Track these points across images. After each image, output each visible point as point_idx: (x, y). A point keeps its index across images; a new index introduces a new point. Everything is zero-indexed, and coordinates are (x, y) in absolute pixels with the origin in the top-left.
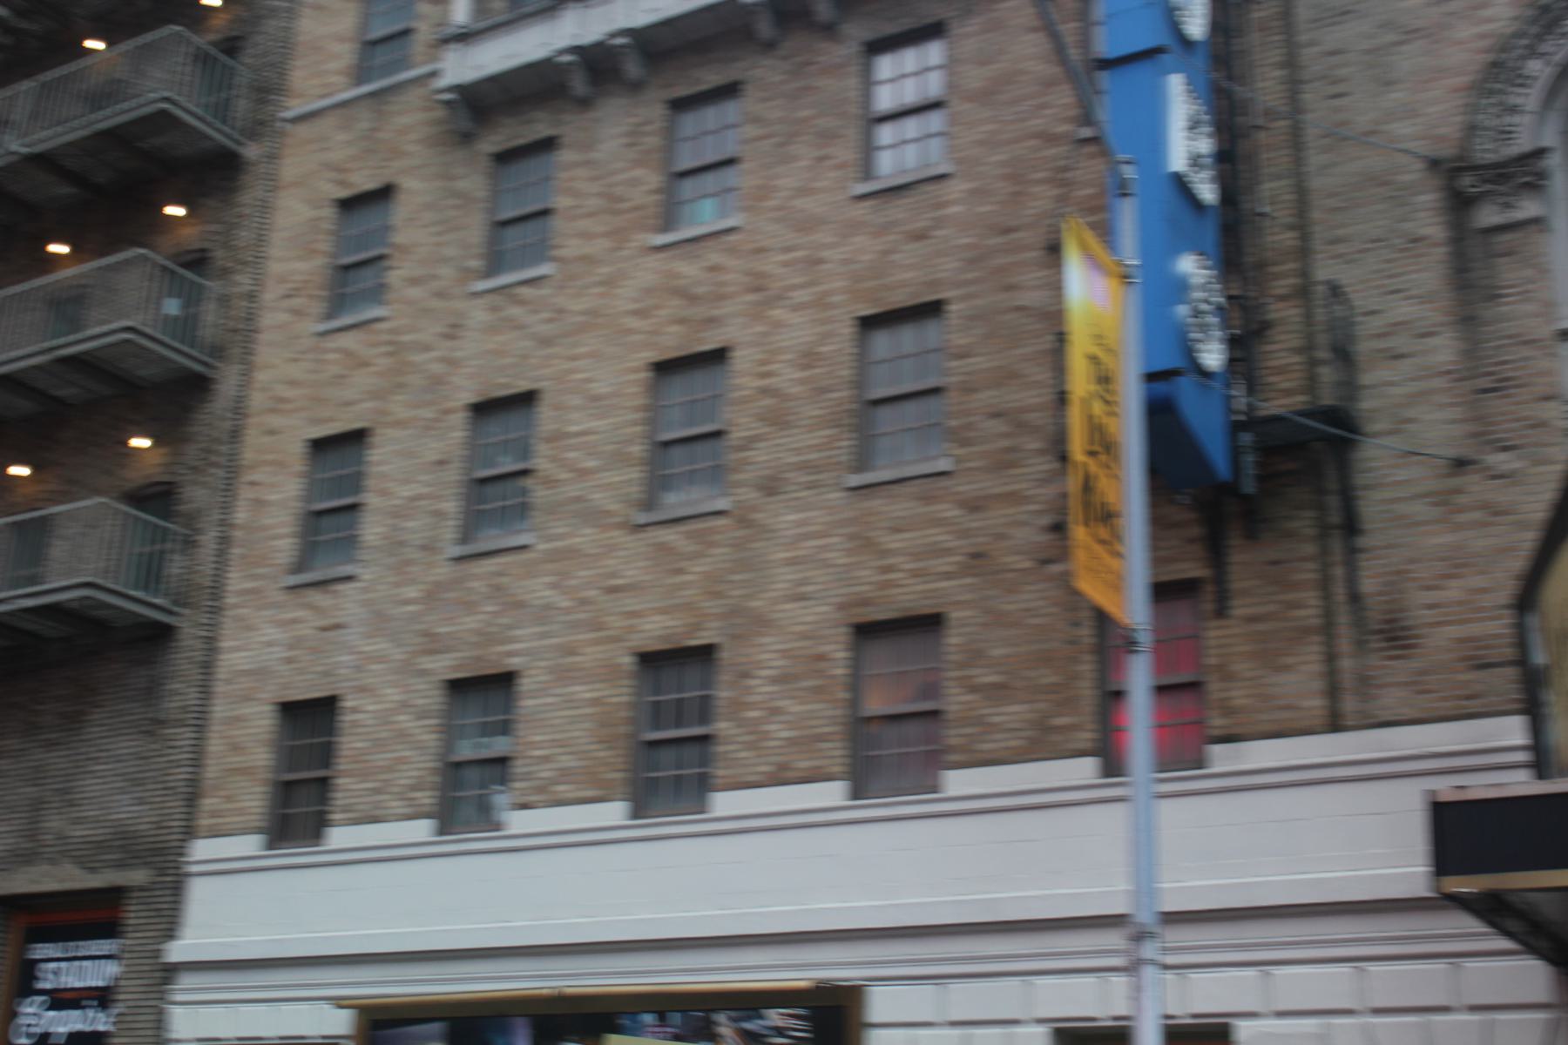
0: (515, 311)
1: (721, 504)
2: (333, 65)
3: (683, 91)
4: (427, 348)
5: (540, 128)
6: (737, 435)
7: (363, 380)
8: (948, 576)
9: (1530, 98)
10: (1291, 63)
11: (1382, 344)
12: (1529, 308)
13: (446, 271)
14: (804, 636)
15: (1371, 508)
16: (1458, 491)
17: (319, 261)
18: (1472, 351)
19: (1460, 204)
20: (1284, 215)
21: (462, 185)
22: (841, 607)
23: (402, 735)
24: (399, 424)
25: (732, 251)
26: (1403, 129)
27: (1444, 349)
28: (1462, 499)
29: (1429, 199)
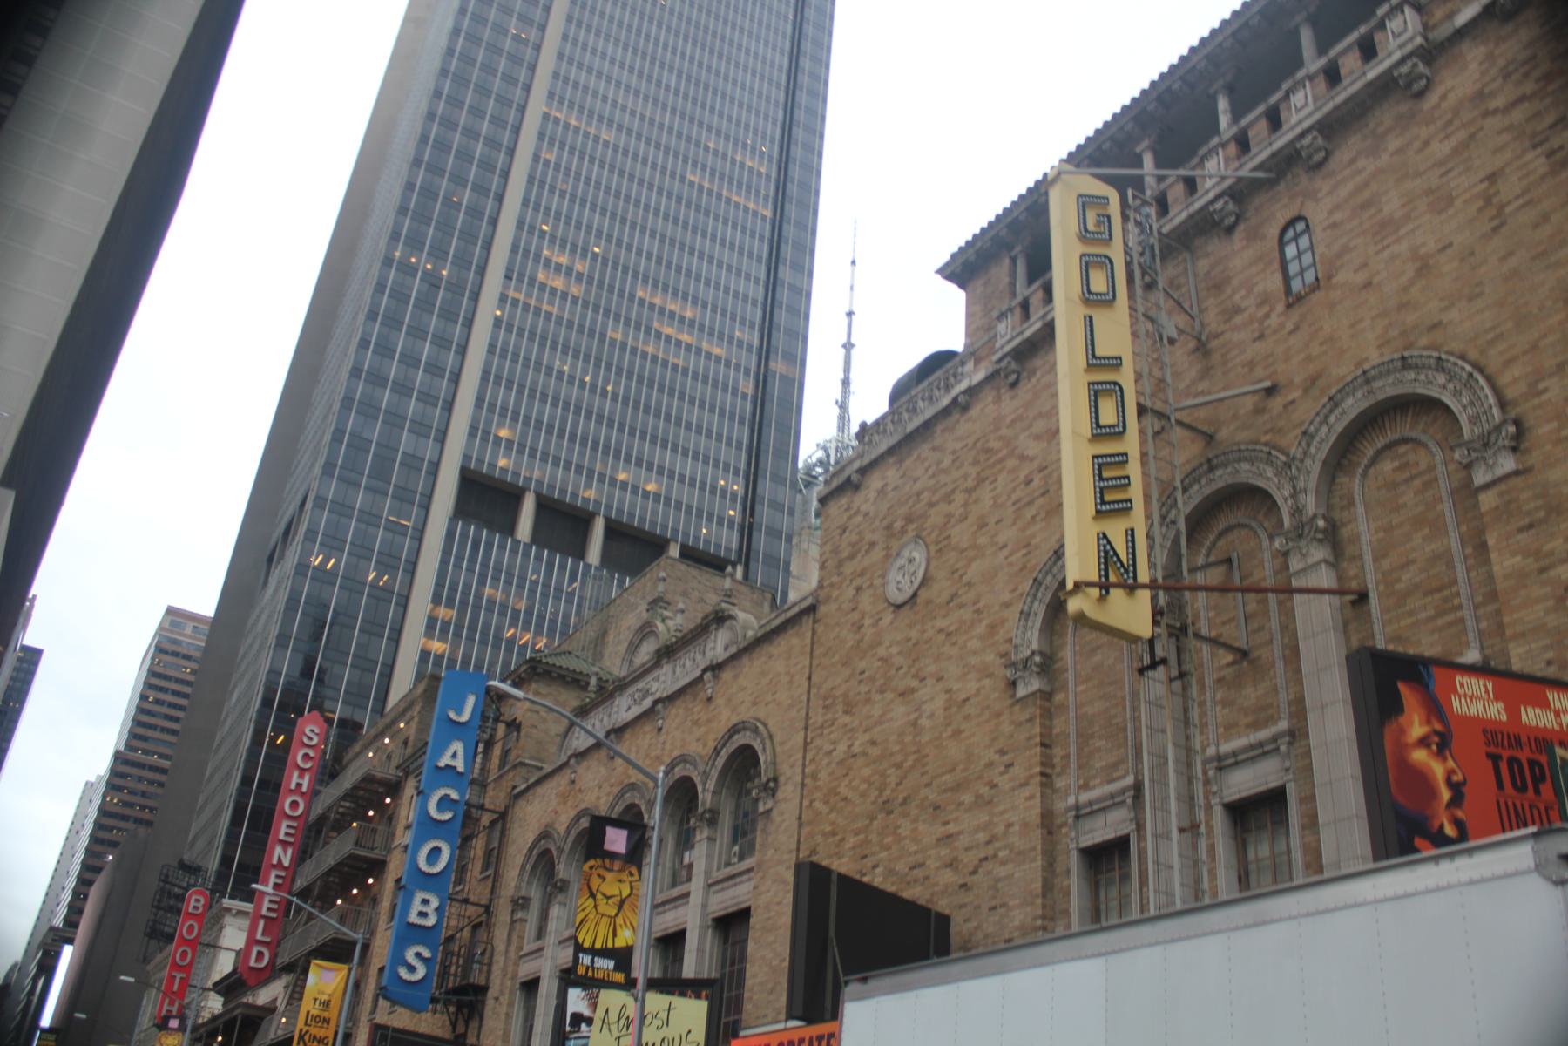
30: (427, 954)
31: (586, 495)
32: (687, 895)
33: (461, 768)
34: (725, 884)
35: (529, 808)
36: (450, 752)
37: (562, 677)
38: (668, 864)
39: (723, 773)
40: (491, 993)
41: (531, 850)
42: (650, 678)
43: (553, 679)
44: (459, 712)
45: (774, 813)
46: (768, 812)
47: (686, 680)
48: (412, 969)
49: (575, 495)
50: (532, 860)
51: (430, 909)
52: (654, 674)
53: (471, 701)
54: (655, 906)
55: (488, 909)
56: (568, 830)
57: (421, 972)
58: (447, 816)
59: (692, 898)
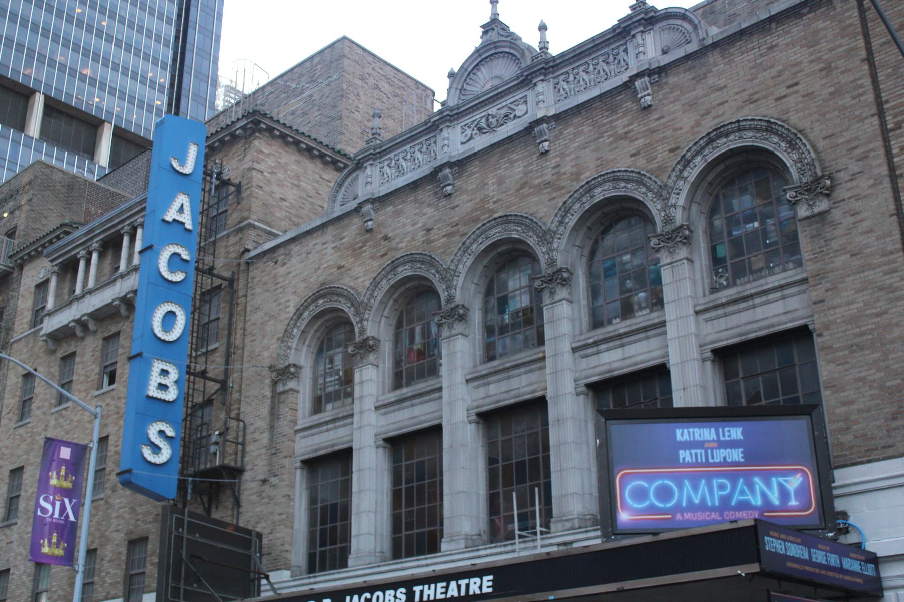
0: (61, 420)
1: (102, 496)
2: (25, 320)
3: (106, 334)
4: (40, 435)
5: (72, 349)
6: (108, 469)
7: (24, 447)
8: (150, 522)
9: (294, 343)
10: (244, 329)
11: (252, 436)
12: (285, 423)
13: (46, 404)
14: (117, 545)
15: (244, 498)
16: (264, 491)
17: (17, 399)
18: (271, 440)
19: (275, 383)
20: (236, 387)
21: (53, 370)
22: (126, 534)
23: (23, 583)
24: (31, 464)
25: (113, 398)
26: (266, 354)
27: (265, 439)
28: (264, 494)
29: (268, 381)
30: (170, 432)
31: (27, 72)
32: (663, 324)
33: (189, 226)
34: (729, 309)
35: (281, 270)
36: (176, 206)
37: (283, 137)
38: (583, 302)
39: (696, 185)
40: (247, 476)
41: (299, 313)
42: (509, 99)
43: (274, 137)
44: (183, 163)
45: (836, 214)
46: (822, 214)
47: (595, 92)
48: (156, 449)
49: (16, 71)
50: (302, 324)
51: (169, 381)
52: (518, 96)
53: (193, 151)
54: (574, 350)
55: (224, 384)
56: (375, 283)
57: (165, 455)
58: (178, 277)
59: (671, 329)
